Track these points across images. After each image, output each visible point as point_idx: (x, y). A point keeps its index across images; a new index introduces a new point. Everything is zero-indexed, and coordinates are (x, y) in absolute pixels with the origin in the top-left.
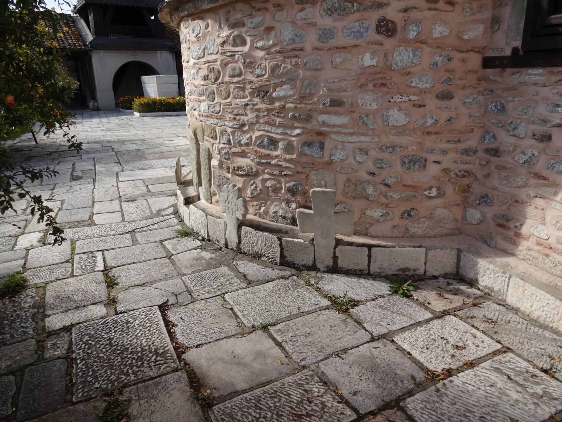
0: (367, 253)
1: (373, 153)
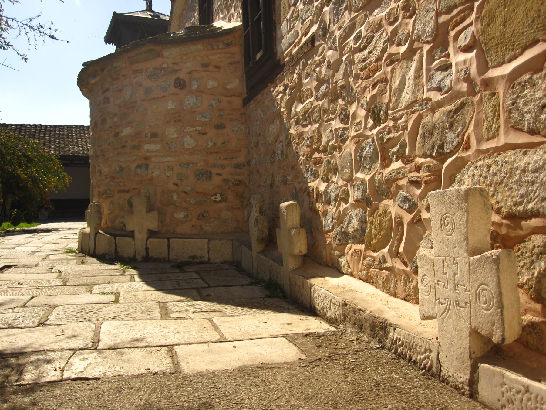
0: (167, 243)
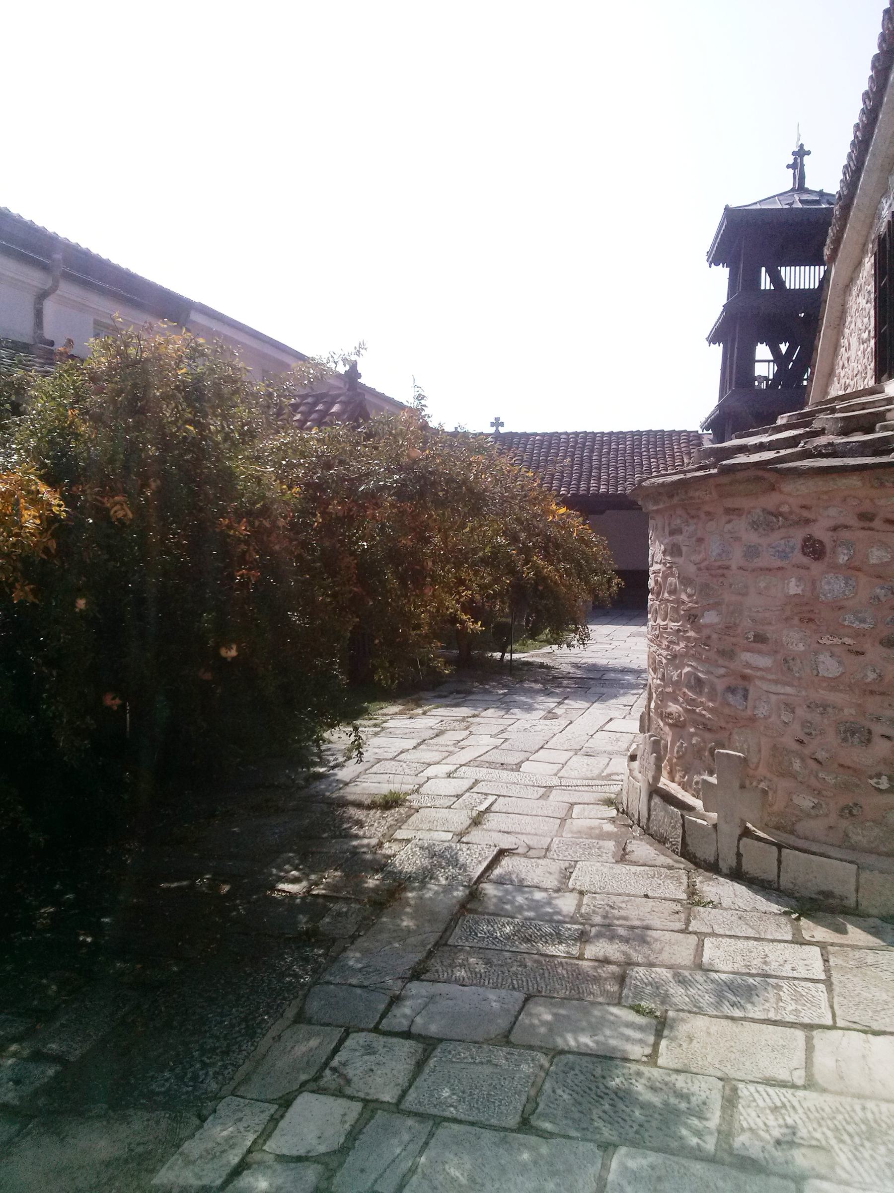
1: (799, 712)
